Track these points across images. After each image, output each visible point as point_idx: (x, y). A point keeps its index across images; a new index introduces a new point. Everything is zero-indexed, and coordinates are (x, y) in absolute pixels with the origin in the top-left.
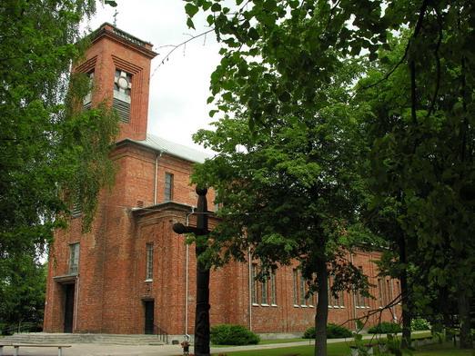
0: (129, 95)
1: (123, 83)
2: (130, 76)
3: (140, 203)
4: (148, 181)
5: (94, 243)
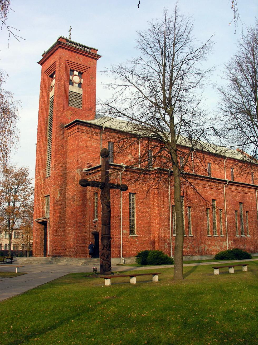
0: (81, 87)
1: (76, 79)
2: (80, 73)
3: (90, 165)
4: (96, 148)
5: (59, 195)
